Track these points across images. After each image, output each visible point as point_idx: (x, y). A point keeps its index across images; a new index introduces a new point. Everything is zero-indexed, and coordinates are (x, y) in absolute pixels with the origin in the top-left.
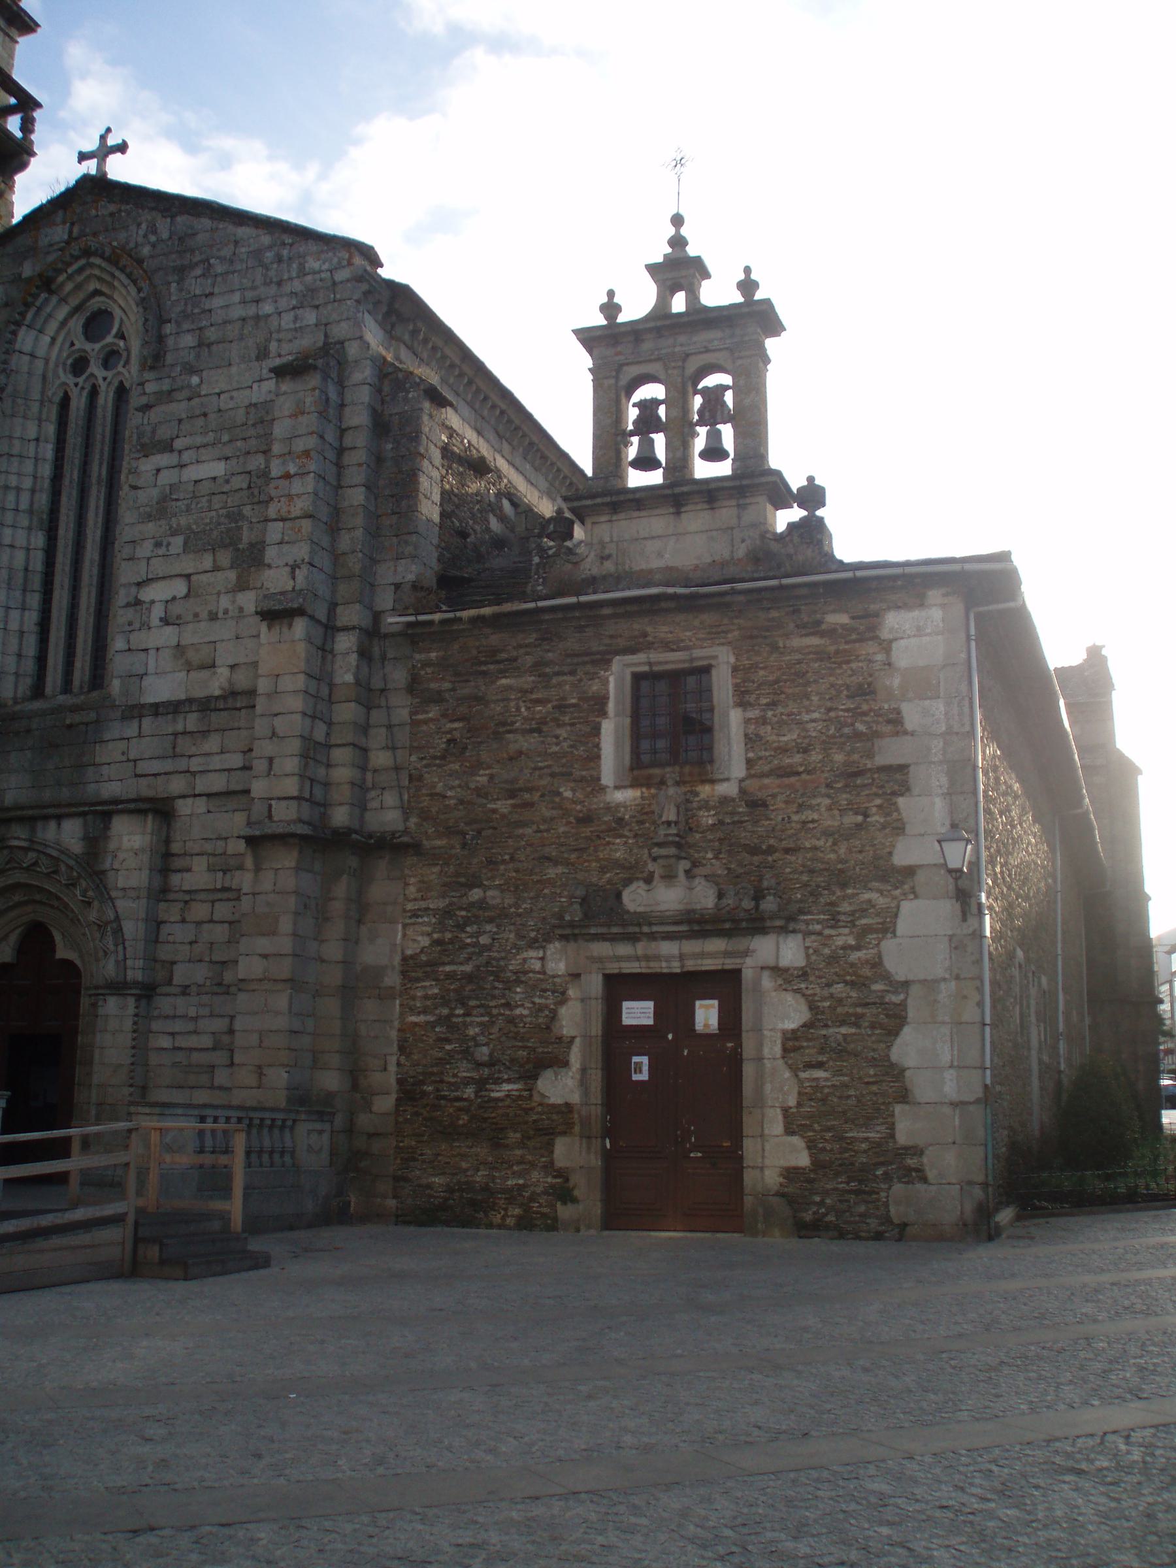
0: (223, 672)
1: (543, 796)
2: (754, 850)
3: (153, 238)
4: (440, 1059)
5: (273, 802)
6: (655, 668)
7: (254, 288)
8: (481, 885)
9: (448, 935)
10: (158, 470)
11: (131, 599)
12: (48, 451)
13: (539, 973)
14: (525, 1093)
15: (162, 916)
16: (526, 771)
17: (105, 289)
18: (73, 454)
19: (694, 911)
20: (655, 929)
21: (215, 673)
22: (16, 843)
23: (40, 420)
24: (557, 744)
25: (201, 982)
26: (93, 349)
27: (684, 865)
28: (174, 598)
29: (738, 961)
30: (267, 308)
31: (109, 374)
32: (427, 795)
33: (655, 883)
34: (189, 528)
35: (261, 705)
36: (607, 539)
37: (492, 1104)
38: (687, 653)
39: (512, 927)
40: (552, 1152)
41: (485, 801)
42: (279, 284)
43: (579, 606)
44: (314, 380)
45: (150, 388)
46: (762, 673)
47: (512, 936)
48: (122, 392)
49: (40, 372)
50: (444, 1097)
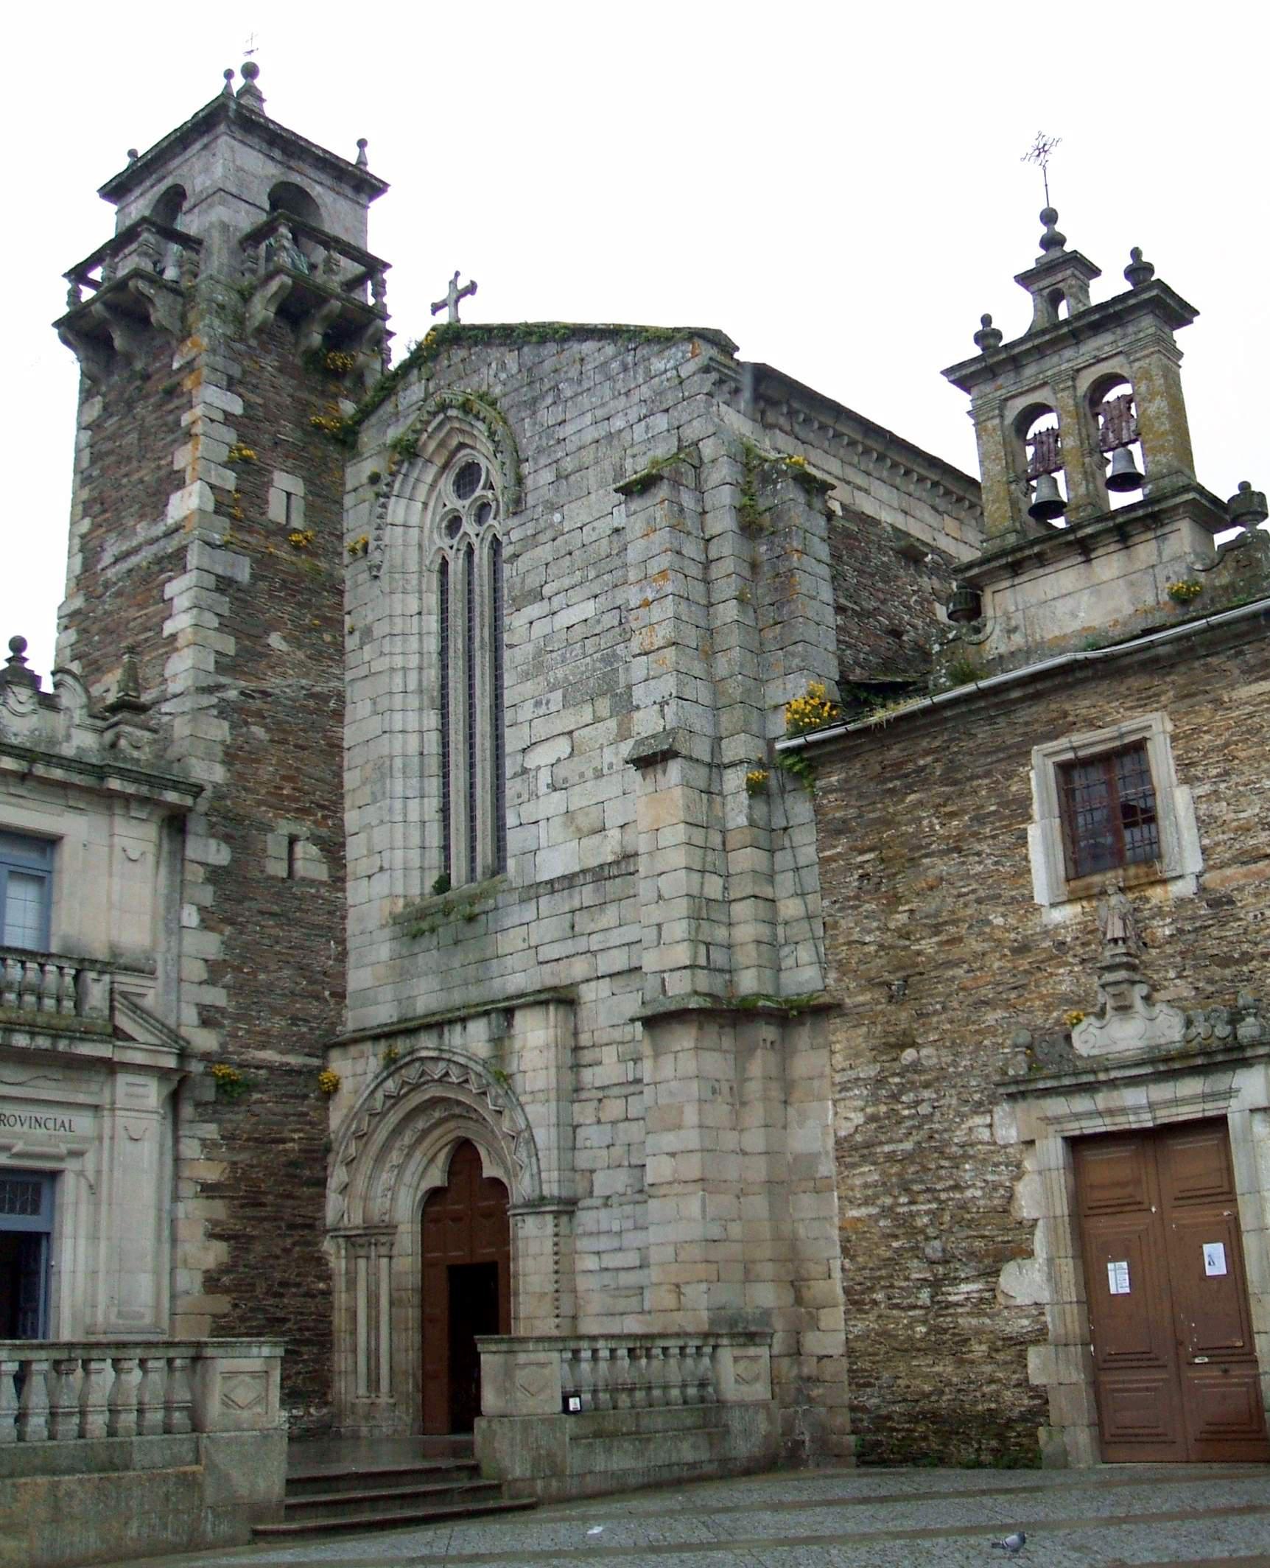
0: (614, 834)
1: (971, 927)
2: (1225, 961)
3: (503, 376)
4: (889, 1259)
5: (666, 975)
6: (1081, 753)
7: (603, 405)
8: (914, 1044)
9: (883, 1109)
10: (531, 623)
11: (518, 769)
12: (433, 623)
13: (988, 1143)
14: (987, 1295)
15: (578, 1119)
16: (949, 900)
17: (468, 441)
18: (457, 623)
19: (1158, 1047)
20: (1114, 1074)
21: (606, 836)
22: (424, 1054)
23: (420, 592)
24: (980, 863)
25: (621, 1189)
26: (462, 505)
27: (1142, 990)
28: (559, 760)
29: (1221, 1104)
30: (618, 423)
31: (482, 530)
32: (844, 944)
33: (1108, 1016)
34: (566, 678)
35: (643, 865)
36: (1012, 608)
37: (951, 1311)
38: (1115, 728)
39: (953, 1092)
40: (1026, 1366)
41: (907, 943)
42: (627, 394)
43: (982, 694)
44: (663, 491)
45: (515, 536)
46: (1207, 737)
47: (954, 1101)
48: (496, 545)
49: (414, 541)
50: (897, 1306)
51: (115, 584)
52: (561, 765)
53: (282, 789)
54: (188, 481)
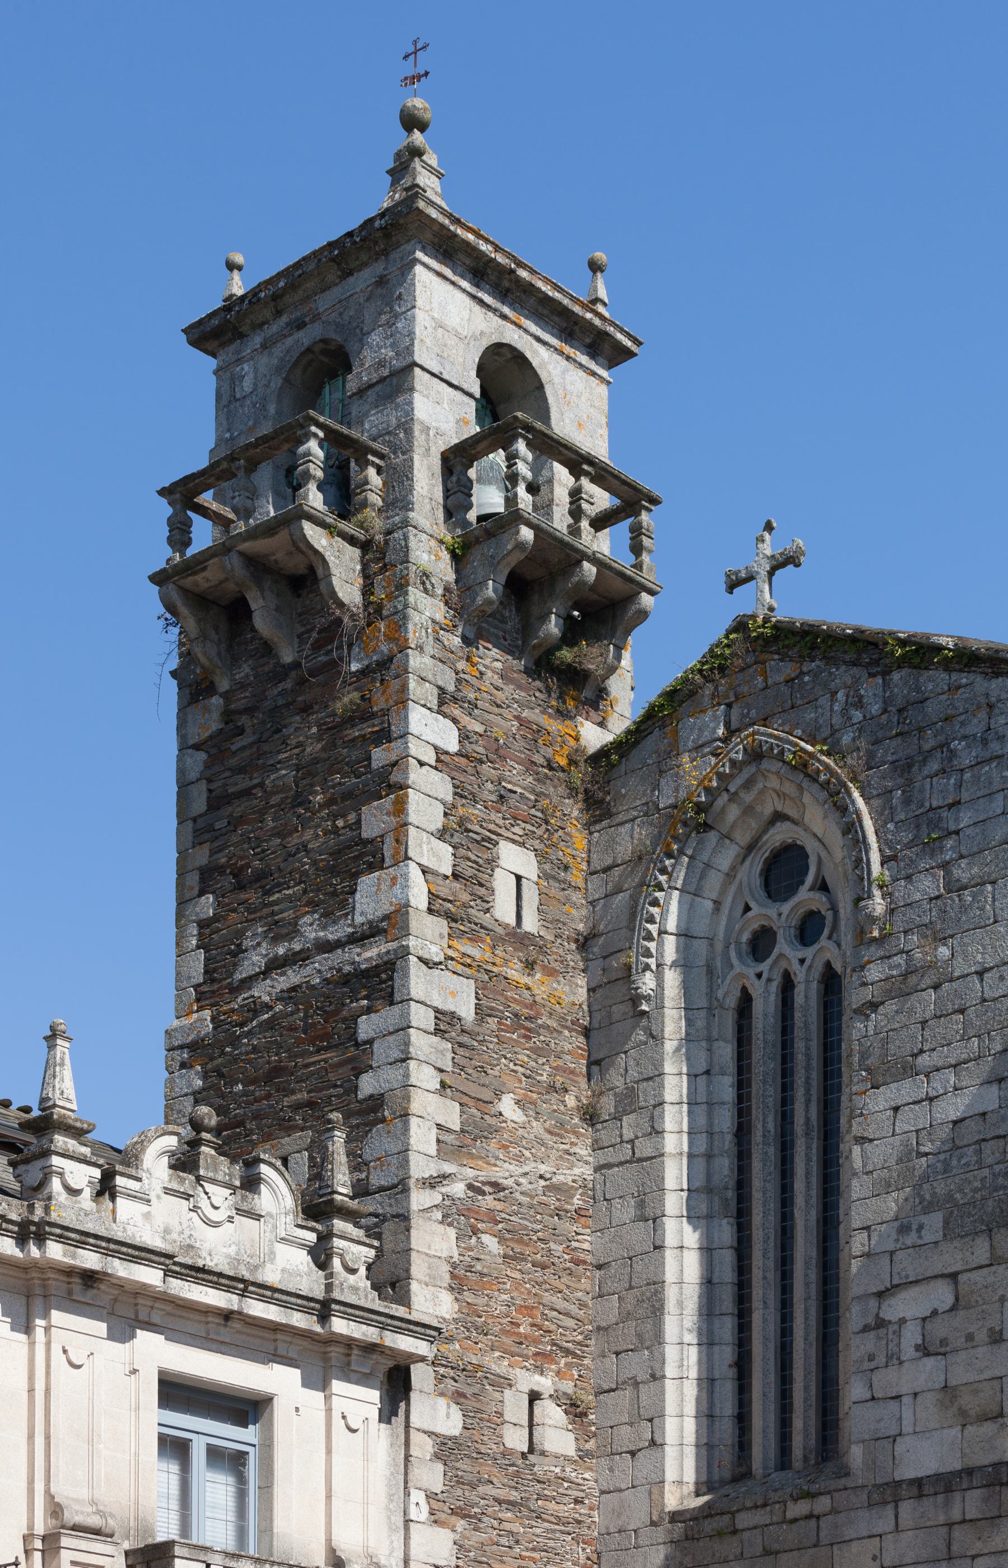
10: (896, 1109)
11: (871, 1320)
28: (935, 1313)
51: (269, 1007)
52: (939, 1319)
53: (518, 1325)
54: (388, 862)
